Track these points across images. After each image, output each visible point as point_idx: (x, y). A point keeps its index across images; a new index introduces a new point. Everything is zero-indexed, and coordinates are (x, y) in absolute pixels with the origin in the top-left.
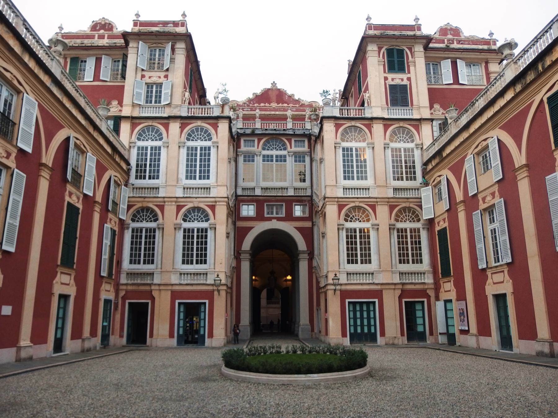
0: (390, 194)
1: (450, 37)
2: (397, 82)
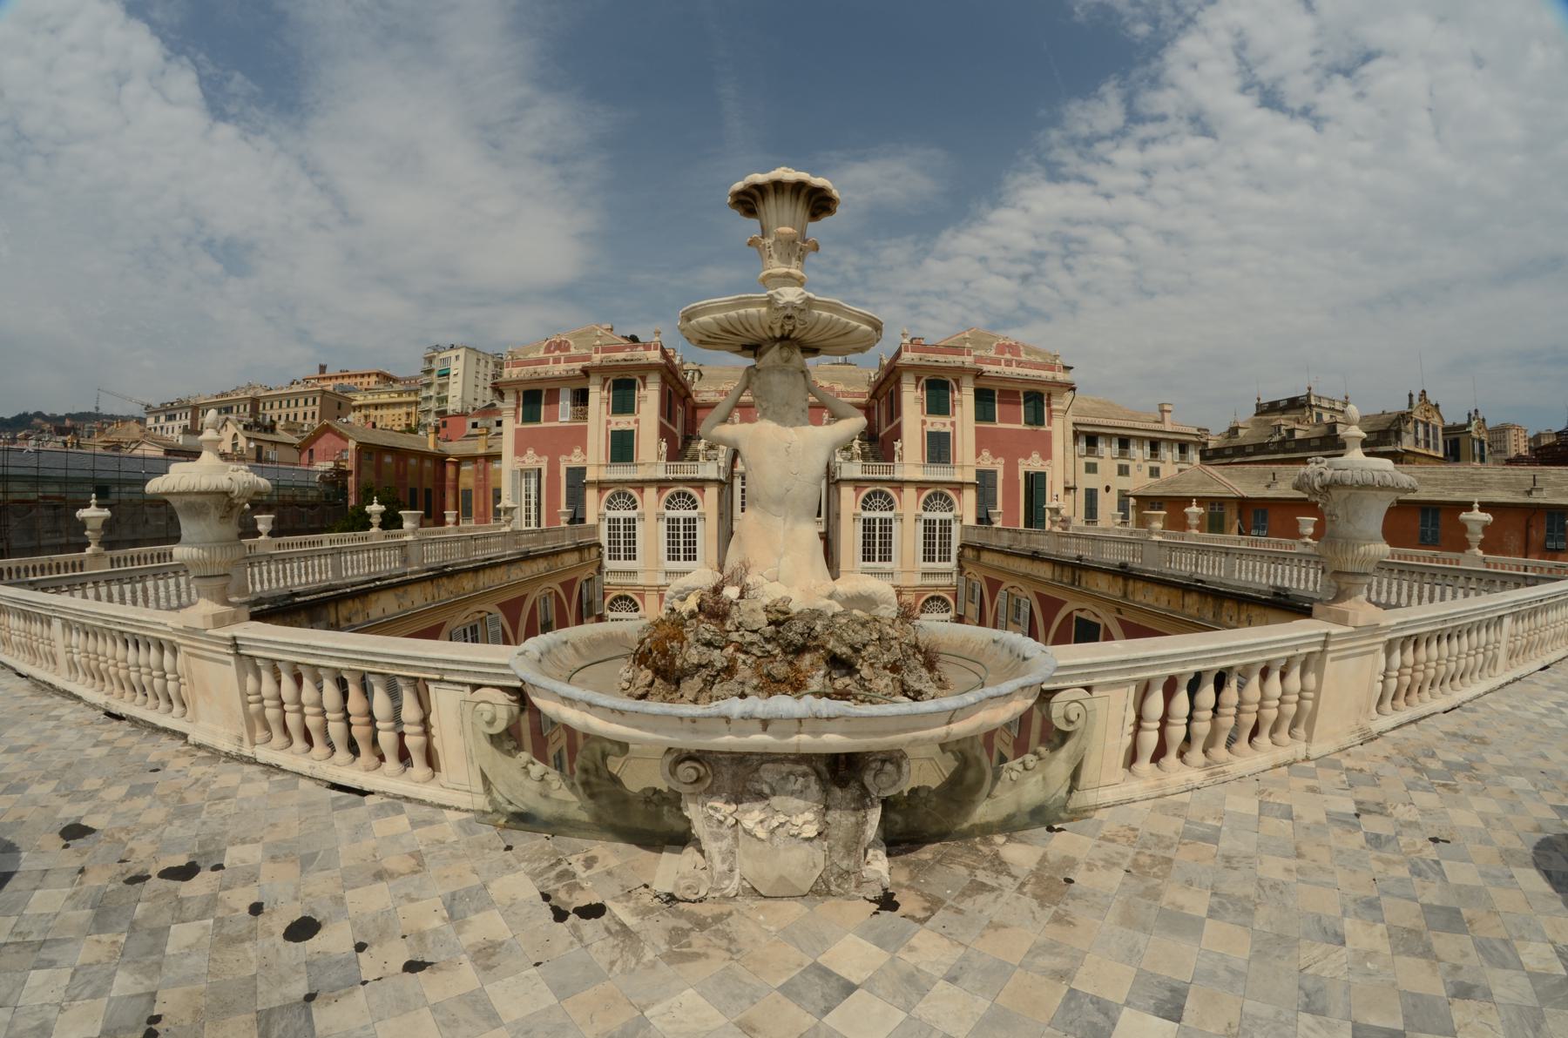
0: (917, 580)
1: (1008, 356)
2: (938, 428)
